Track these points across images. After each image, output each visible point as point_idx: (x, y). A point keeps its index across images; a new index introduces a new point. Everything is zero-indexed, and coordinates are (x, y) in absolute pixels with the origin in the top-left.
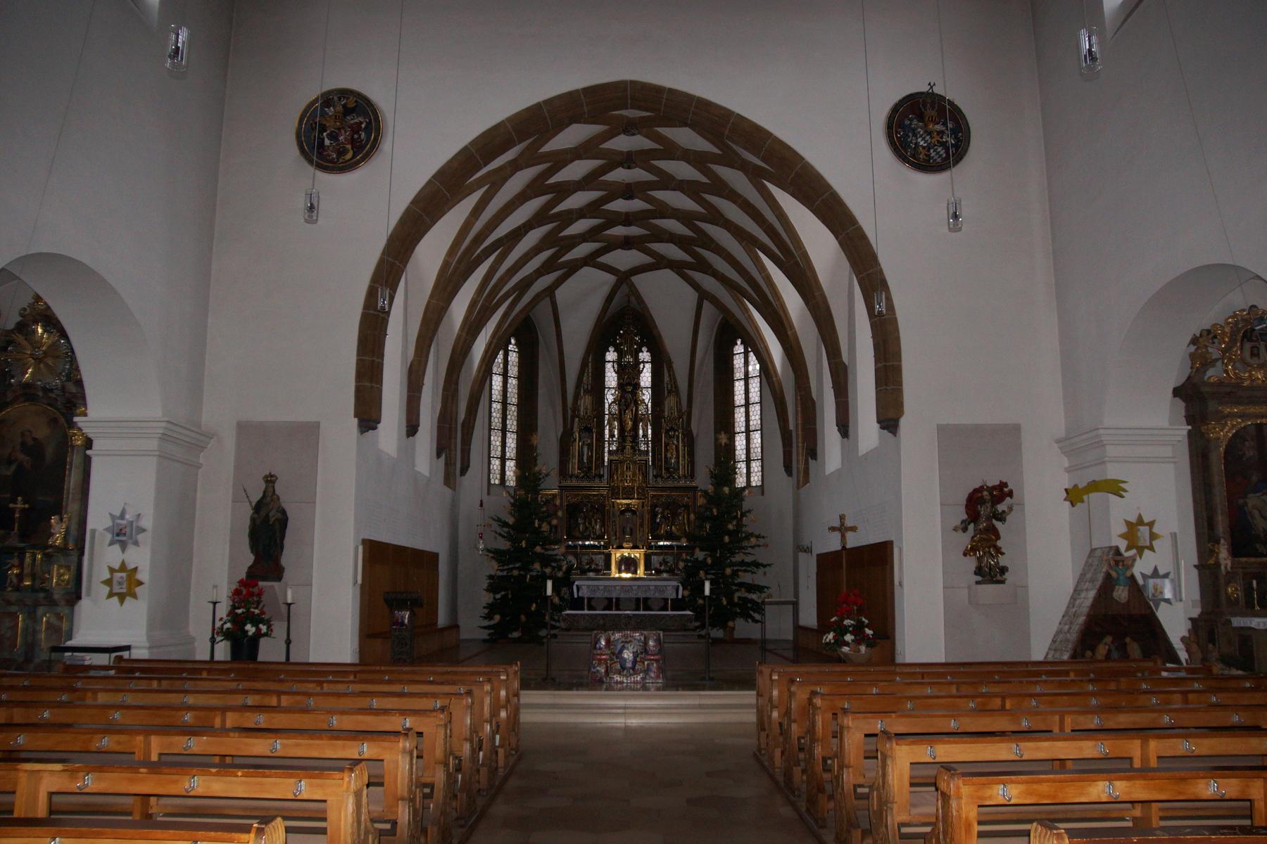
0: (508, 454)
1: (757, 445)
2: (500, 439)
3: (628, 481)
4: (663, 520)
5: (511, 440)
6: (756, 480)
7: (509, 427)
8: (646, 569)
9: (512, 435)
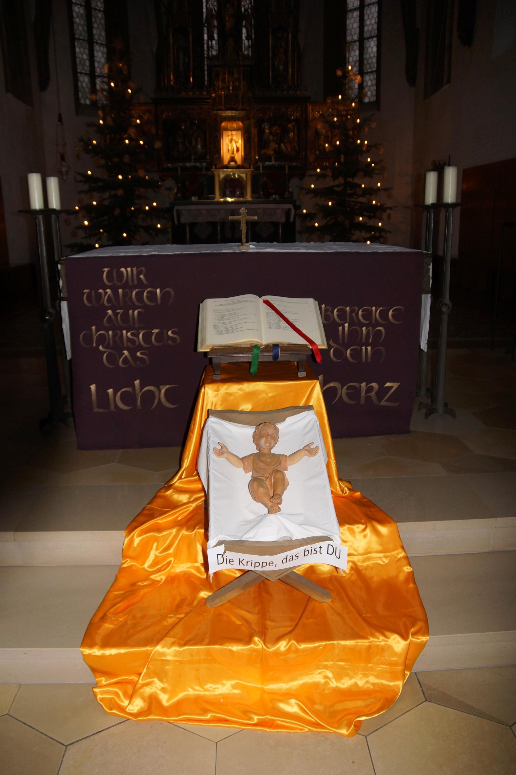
0: (98, 71)
1: (372, 55)
2: (87, 51)
3: (231, 88)
4: (271, 138)
5: (100, 54)
6: (370, 96)
7: (96, 37)
8: (253, 192)
9: (102, 48)
